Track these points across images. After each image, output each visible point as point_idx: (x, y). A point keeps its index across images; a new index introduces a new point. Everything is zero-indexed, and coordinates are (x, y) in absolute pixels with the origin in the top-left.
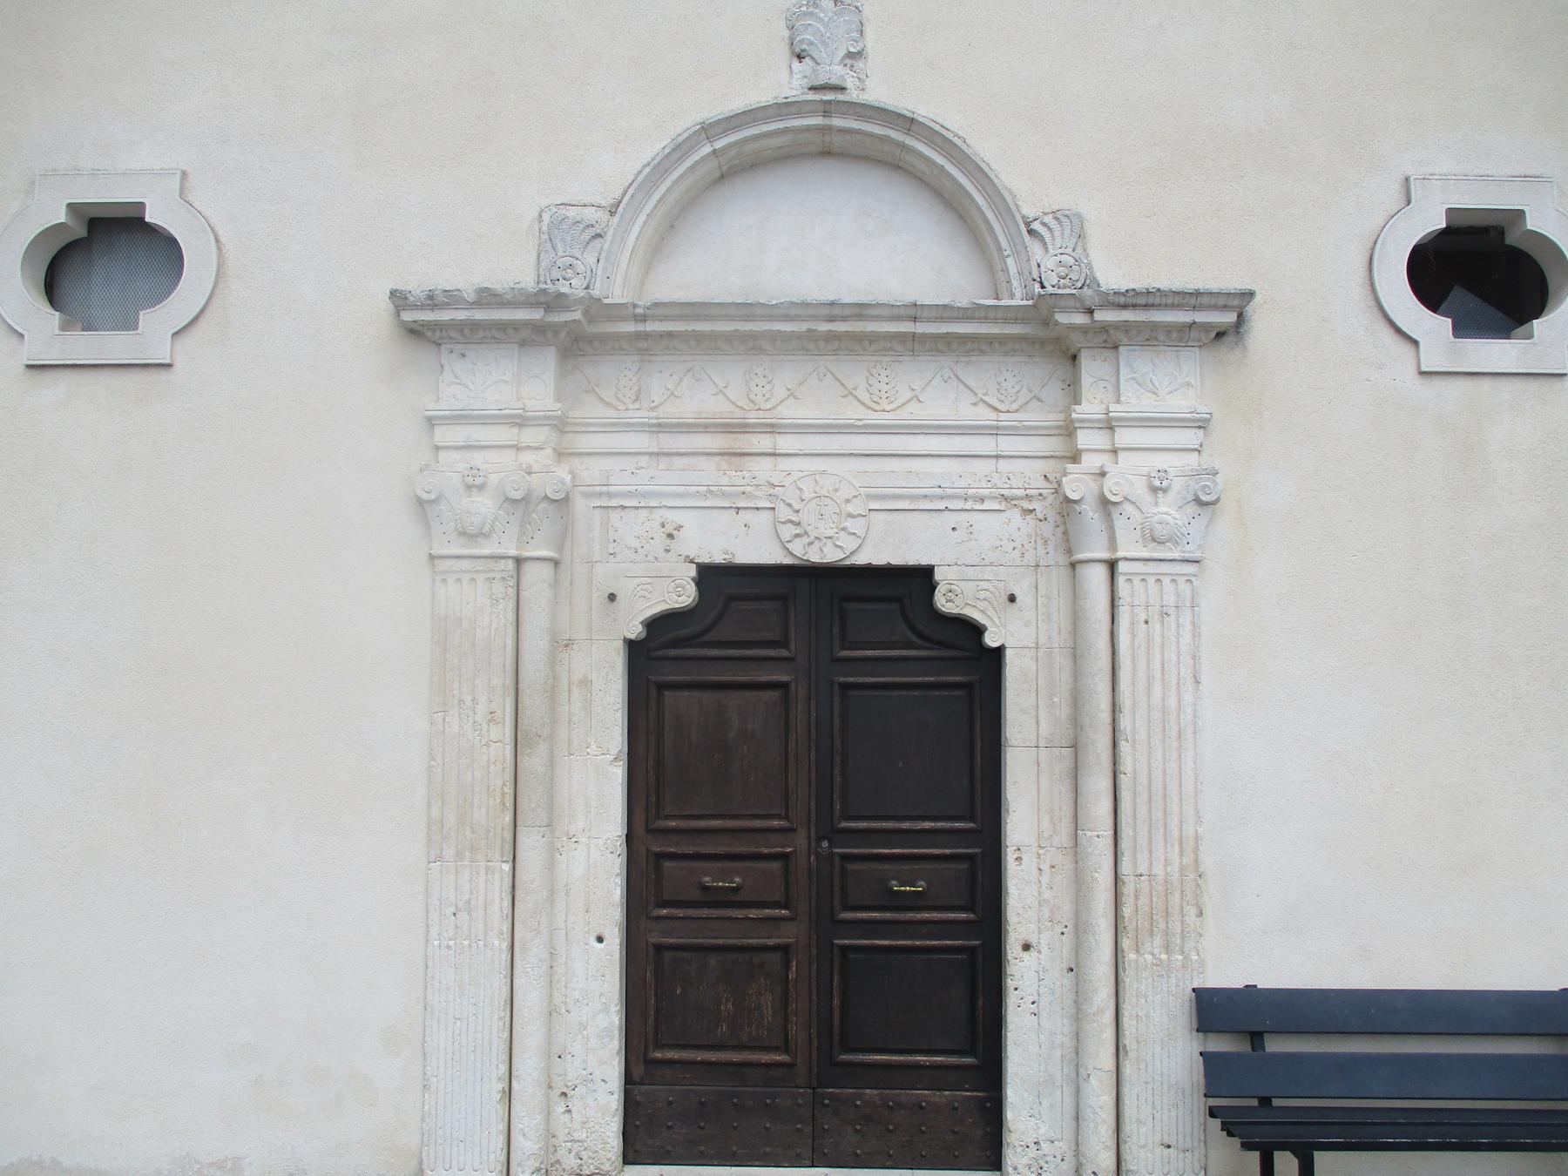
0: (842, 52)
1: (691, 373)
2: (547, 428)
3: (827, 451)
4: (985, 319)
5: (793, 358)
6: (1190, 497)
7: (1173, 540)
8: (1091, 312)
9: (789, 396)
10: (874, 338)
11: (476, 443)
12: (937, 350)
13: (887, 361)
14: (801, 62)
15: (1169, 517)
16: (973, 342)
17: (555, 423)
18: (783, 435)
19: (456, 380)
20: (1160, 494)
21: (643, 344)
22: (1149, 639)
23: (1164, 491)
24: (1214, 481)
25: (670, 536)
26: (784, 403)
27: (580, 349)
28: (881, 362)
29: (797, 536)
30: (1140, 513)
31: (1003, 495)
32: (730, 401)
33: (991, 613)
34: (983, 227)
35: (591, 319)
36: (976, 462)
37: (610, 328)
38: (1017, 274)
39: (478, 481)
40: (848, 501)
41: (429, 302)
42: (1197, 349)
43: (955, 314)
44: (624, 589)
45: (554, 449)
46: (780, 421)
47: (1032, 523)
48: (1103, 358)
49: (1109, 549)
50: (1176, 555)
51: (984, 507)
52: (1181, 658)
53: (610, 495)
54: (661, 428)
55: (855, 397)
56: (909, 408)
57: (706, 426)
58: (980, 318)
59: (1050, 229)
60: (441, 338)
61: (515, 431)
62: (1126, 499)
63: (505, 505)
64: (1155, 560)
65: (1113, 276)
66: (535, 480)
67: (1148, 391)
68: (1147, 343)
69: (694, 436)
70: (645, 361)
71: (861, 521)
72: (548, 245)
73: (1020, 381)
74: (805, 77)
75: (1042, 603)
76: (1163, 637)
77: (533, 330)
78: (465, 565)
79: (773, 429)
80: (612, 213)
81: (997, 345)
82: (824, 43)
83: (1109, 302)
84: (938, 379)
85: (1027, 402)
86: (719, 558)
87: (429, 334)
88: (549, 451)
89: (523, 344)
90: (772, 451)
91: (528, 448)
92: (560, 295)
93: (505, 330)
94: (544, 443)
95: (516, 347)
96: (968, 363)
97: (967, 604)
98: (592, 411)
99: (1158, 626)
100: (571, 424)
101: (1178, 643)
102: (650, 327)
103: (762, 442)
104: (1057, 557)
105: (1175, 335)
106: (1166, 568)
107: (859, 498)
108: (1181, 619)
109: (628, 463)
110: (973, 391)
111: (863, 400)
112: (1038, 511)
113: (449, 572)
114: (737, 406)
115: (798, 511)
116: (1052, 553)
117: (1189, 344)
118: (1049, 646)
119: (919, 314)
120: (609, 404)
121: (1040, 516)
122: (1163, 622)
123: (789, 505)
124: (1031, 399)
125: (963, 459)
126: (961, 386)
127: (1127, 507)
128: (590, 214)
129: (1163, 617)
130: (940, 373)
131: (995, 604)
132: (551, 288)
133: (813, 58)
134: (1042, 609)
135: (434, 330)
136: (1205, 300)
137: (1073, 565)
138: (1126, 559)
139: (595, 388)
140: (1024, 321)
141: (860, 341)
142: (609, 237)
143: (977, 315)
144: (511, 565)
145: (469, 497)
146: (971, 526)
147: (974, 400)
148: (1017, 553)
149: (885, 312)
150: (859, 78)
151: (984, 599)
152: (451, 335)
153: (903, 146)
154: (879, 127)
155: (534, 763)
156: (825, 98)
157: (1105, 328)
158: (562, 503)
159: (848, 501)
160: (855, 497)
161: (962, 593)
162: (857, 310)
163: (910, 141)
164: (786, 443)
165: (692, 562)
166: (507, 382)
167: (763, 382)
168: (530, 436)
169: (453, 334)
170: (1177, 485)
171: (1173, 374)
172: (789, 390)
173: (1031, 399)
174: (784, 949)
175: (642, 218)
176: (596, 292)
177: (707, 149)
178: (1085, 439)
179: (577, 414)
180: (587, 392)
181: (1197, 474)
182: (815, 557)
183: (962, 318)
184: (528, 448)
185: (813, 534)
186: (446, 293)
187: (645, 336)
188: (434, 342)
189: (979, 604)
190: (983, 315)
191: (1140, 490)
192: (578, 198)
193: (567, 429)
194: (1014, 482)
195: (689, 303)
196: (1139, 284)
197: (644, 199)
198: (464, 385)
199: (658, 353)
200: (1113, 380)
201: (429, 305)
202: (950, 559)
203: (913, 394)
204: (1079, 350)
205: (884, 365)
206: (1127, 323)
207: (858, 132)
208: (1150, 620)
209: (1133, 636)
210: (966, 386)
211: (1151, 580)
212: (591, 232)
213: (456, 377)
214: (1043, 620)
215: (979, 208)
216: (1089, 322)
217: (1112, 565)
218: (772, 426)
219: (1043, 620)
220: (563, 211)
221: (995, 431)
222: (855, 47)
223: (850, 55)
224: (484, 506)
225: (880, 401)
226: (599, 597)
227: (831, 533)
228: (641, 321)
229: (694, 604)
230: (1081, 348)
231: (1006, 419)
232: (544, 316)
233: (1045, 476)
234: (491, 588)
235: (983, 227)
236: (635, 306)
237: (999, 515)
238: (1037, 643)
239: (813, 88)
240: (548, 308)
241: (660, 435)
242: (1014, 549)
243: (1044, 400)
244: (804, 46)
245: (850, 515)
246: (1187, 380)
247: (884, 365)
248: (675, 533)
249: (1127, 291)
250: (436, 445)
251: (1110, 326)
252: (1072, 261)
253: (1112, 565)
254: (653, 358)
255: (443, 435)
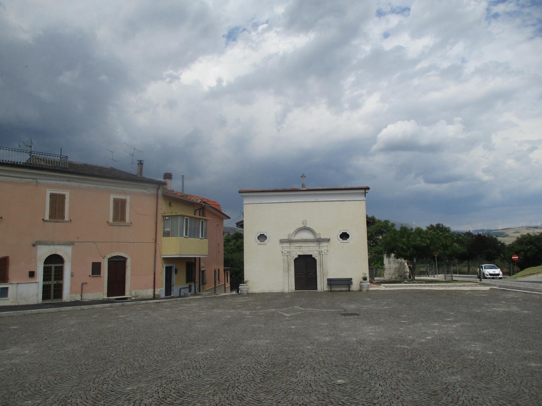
54: (295, 247)
65: (322, 237)
103: (302, 247)
155: (289, 267)
158: (290, 252)
164: (303, 247)
168: (288, 248)
174: (304, 278)
224: (286, 252)
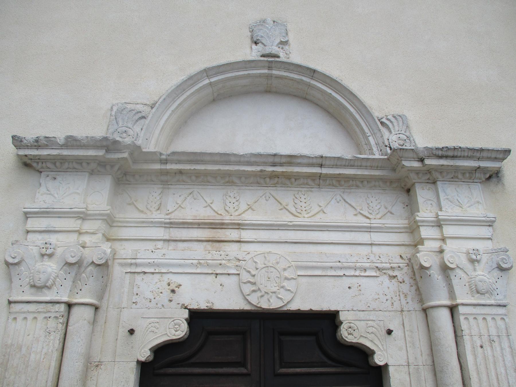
0: (277, 41)
1: (191, 195)
2: (100, 221)
3: (271, 240)
4: (360, 167)
5: (250, 188)
6: (495, 266)
7: (489, 292)
8: (422, 160)
9: (249, 208)
10: (297, 177)
11: (52, 229)
12: (333, 185)
13: (305, 191)
14: (256, 45)
15: (485, 278)
16: (353, 180)
17: (105, 218)
18: (244, 230)
19: (47, 192)
20: (476, 264)
21: (164, 178)
22: (485, 358)
23: (478, 261)
24: (508, 256)
25: (173, 291)
26: (246, 213)
27: (127, 180)
28: (301, 191)
29: (254, 291)
30: (467, 276)
31: (377, 267)
32: (214, 211)
33: (377, 342)
34: (353, 123)
35: (135, 162)
36: (360, 248)
37: (146, 167)
38: (375, 145)
39: (49, 252)
40: (285, 270)
41: (36, 144)
42: (479, 184)
43: (344, 163)
44: (140, 326)
45: (103, 235)
46: (244, 221)
47: (396, 284)
48: (427, 188)
49: (449, 299)
50: (492, 302)
51: (367, 274)
52: (508, 371)
53: (136, 265)
54: (171, 225)
55: (287, 210)
56: (318, 216)
57: (199, 224)
58: (358, 166)
59: (391, 122)
60: (42, 168)
61: (79, 222)
62: (458, 267)
63: (64, 267)
64: (489, 305)
66: (87, 251)
67: (457, 206)
68: (452, 180)
69: (191, 230)
70: (165, 188)
71: (293, 282)
72: (114, 122)
73: (380, 203)
74: (259, 51)
75: (408, 335)
76: (494, 356)
77: (98, 164)
78: (32, 307)
79: (239, 226)
80: (152, 108)
81: (365, 183)
82: (268, 37)
83: (433, 154)
84: (334, 201)
85: (385, 215)
86: (203, 306)
87: (35, 165)
88: (100, 235)
89: (92, 173)
90: (239, 239)
91: (87, 233)
92: (115, 142)
93: (81, 164)
94: (97, 230)
95: (87, 174)
96: (350, 193)
97: (361, 336)
98: (132, 215)
99: (489, 349)
100: (117, 221)
101: (504, 361)
102: (169, 167)
103: (233, 234)
104: (413, 305)
105: (467, 175)
106: (486, 310)
107: (292, 267)
108: (502, 344)
109: (150, 246)
110: (354, 208)
111: (292, 211)
112: (399, 277)
113: (19, 312)
114: (218, 214)
115: (254, 276)
116: (410, 302)
117: (475, 181)
118: (416, 364)
119: (324, 163)
120: (142, 212)
121: (401, 280)
122: (492, 346)
123: (249, 272)
124: (387, 213)
125: (351, 246)
126: (347, 205)
127: (458, 271)
128: (140, 108)
129: (491, 343)
130: (335, 197)
131: (379, 336)
132: (111, 137)
133: (263, 44)
134: (408, 339)
135: (38, 163)
136: (485, 154)
137: (425, 310)
138: (463, 305)
139: (134, 202)
140: (381, 168)
141: (290, 179)
142: (149, 118)
143: (356, 164)
144: (62, 308)
145: (42, 262)
146: (360, 286)
147: (355, 213)
148: (389, 302)
149: (305, 161)
150: (286, 53)
151: (372, 333)
152: (48, 166)
153: (309, 85)
154: (297, 75)
156: (269, 60)
157: (429, 171)
159: (285, 270)
160: (289, 267)
161: (358, 329)
162: (288, 159)
163: (313, 82)
164: (246, 235)
165: (186, 308)
166: (78, 194)
167: (234, 200)
168: (88, 226)
169: (49, 165)
170: (485, 258)
171: (468, 197)
172: (248, 205)
173: (387, 213)
175: (169, 112)
176: (139, 142)
177: (207, 81)
178: (425, 232)
179: (121, 216)
180: (130, 204)
181: (496, 252)
182: (265, 305)
183: (348, 166)
184: (87, 233)
185: (263, 290)
186: (47, 139)
187: (166, 173)
188: (38, 171)
189: (368, 336)
190: (359, 164)
191: (463, 261)
192: (134, 101)
193: (115, 224)
194: (383, 259)
195: (193, 153)
196: (451, 144)
197: (171, 102)
198: (52, 195)
199: (173, 183)
200: (435, 200)
201: (35, 146)
202: (348, 307)
203: (320, 209)
204: (413, 184)
205: (303, 193)
206: (443, 167)
207: (286, 78)
208: (484, 345)
209: (475, 356)
210: (350, 205)
211: (480, 318)
212: (140, 115)
213: (48, 190)
214: (410, 347)
215: (351, 114)
216: (421, 166)
217: (453, 309)
218: (239, 224)
219: (410, 347)
220: (126, 105)
221: (369, 229)
222: (284, 39)
223: (282, 43)
225: (301, 212)
226: (123, 332)
227: (274, 289)
228: (164, 163)
229: (186, 337)
230: (415, 183)
231: (376, 222)
232: (105, 154)
233: (401, 256)
234: (47, 325)
235: (353, 123)
236: (161, 154)
237: (375, 279)
238: (408, 361)
239: (263, 56)
240: (108, 150)
241: (171, 229)
242: (387, 300)
243: (394, 213)
244: (258, 38)
245: (287, 279)
246: (477, 200)
247: (303, 193)
248: (176, 289)
249: (443, 148)
250: (27, 230)
251: (433, 169)
252: (405, 138)
253: (453, 309)
254: (170, 186)
255: (33, 224)
